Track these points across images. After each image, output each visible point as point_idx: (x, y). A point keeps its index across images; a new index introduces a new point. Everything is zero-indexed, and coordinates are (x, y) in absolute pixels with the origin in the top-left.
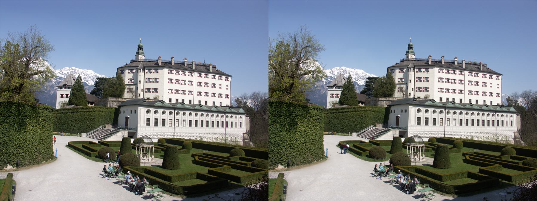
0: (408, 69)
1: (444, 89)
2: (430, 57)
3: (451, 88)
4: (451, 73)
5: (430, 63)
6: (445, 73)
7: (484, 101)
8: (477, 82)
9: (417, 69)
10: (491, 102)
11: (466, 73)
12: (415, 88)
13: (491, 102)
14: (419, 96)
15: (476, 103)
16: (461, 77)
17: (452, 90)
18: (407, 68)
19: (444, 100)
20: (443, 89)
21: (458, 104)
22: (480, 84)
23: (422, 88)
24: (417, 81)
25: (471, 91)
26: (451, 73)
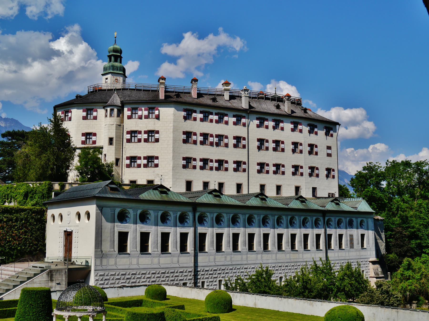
0: (107, 110)
1: (198, 160)
2: (161, 81)
3: (214, 158)
7: (297, 189)
9: (128, 110)
10: (314, 189)
12: (124, 157)
13: (314, 189)
14: (133, 179)
15: (278, 193)
16: (240, 131)
18: (104, 108)
19: (197, 187)
21: (232, 196)
23: (142, 158)
24: (129, 141)
25: (262, 165)
26: (214, 121)
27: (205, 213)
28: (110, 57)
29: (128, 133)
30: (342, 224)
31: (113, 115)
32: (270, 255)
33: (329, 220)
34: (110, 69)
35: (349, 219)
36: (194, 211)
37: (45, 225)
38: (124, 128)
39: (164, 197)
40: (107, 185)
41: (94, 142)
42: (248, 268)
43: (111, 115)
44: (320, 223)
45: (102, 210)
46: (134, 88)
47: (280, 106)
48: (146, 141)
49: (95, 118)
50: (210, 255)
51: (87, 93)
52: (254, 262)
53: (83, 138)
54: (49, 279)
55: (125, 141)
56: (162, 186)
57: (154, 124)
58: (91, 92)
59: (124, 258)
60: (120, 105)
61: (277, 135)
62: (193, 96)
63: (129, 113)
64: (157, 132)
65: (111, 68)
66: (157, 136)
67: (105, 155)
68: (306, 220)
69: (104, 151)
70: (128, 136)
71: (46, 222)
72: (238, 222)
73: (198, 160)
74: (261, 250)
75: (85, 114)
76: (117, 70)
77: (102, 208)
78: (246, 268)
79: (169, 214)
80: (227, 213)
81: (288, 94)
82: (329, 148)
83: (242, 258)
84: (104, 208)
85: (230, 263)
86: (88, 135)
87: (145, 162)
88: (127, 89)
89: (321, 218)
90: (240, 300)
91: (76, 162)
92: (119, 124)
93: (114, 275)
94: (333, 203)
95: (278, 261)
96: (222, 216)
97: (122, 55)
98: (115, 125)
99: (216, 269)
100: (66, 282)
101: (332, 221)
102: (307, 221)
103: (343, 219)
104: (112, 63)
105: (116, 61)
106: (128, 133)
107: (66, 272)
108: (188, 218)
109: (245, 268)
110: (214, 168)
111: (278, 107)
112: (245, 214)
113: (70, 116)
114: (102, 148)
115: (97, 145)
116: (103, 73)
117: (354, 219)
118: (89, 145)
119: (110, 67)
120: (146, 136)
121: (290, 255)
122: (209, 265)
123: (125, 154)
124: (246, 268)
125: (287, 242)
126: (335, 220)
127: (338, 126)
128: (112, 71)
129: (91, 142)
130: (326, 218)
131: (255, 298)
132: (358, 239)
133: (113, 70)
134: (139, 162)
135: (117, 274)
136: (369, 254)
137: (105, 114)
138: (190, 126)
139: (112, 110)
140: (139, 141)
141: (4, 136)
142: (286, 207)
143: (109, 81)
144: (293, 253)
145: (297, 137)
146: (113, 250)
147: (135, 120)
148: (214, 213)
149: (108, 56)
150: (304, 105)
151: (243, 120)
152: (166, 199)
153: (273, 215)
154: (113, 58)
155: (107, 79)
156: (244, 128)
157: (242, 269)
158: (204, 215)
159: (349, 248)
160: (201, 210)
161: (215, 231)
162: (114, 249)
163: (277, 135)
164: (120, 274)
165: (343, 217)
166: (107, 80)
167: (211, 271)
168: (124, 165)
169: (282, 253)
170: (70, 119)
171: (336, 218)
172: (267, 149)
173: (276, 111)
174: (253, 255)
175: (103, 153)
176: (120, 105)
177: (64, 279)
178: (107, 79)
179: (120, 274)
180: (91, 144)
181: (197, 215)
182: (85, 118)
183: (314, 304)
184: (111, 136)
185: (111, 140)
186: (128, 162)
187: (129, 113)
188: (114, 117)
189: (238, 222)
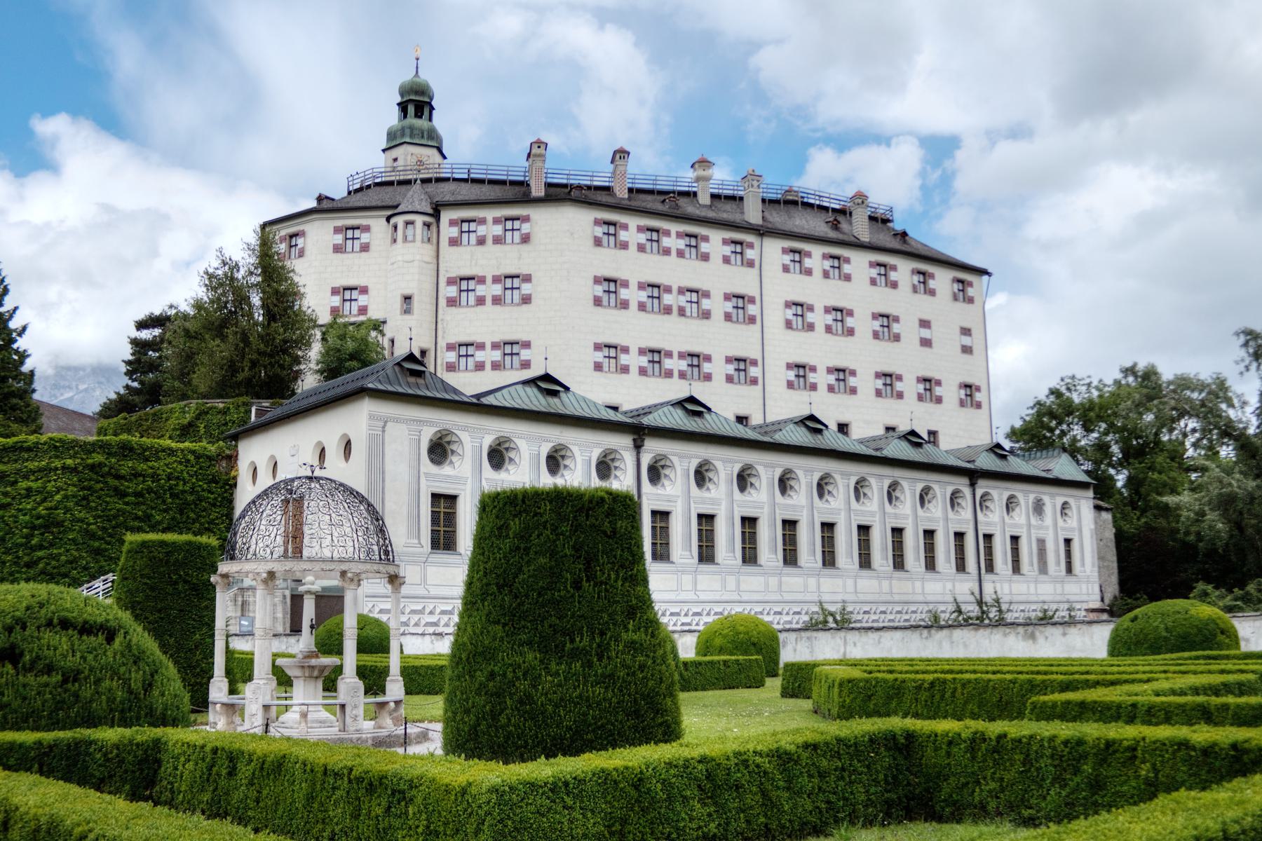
0: (396, 227)
1: (634, 351)
3: (676, 348)
4: (674, 252)
5: (538, 190)
6: (633, 248)
8: (840, 312)
9: (452, 223)
11: (773, 252)
12: (442, 344)
16: (743, 281)
17: (682, 356)
18: (388, 219)
20: (626, 350)
22: (862, 323)
23: (488, 346)
24: (452, 302)
25: (801, 369)
26: (674, 252)
27: (665, 457)
28: (403, 107)
29: (451, 282)
30: (1017, 510)
31: (410, 238)
32: (839, 582)
33: (985, 496)
34: (403, 135)
35: (1035, 498)
36: (638, 447)
37: (232, 494)
38: (440, 269)
39: (554, 405)
40: (398, 364)
41: (363, 310)
42: (785, 612)
43: (405, 239)
44: (963, 504)
45: (384, 427)
46: (465, 176)
47: (839, 222)
48: (497, 300)
49: (365, 248)
50: (683, 572)
51: (345, 194)
52: (799, 597)
53: (336, 301)
54: (239, 614)
55: (442, 302)
56: (547, 378)
57: (519, 258)
58: (357, 191)
59: (446, 565)
60: (430, 211)
61: (835, 293)
62: (618, 193)
63: (454, 232)
64: (527, 279)
65: (408, 132)
66: (526, 288)
67: (392, 341)
68: (927, 494)
69: (389, 330)
70: (452, 291)
71: (235, 485)
72: (756, 488)
73: (634, 351)
74: (815, 565)
75: (339, 239)
76: (423, 137)
77: (386, 422)
78: (780, 613)
79: (569, 454)
80: (724, 461)
81: (859, 192)
82: (966, 332)
83: (767, 585)
84: (389, 424)
85: (735, 597)
86: (345, 291)
87: (497, 355)
88: (446, 180)
89: (967, 491)
90: (795, 650)
91: (315, 351)
92: (428, 259)
93: (421, 612)
94: (993, 456)
95: (862, 597)
96: (712, 467)
97: (433, 103)
98: (416, 263)
99: (699, 610)
100: (284, 624)
101: (992, 500)
102: (930, 496)
103: (1020, 496)
104: (412, 120)
105: (419, 115)
106: (451, 282)
107: (284, 597)
108: (622, 466)
109: (776, 613)
110: (676, 374)
111: (835, 226)
112: (773, 466)
113: (299, 246)
114: (384, 322)
115: (374, 314)
116: (384, 146)
117: (1046, 499)
118: (351, 315)
119: (403, 129)
120: (497, 289)
121: (891, 584)
122: (680, 598)
123: (443, 337)
124: (780, 613)
125: (885, 549)
126: (1001, 499)
127: (985, 278)
128: (408, 140)
129: (355, 310)
130: (979, 492)
131: (845, 640)
132: (1057, 551)
133: (412, 136)
134: (480, 356)
135: (428, 610)
136: (1084, 591)
137: (392, 235)
138: (610, 262)
139: (407, 223)
140: (481, 301)
141: (141, 325)
142: (878, 454)
143: (400, 162)
144: (900, 579)
145: (884, 300)
146: (416, 541)
147: (469, 248)
148: (690, 457)
149: (399, 104)
150: (898, 226)
151: (750, 254)
152: (562, 410)
153: (846, 475)
154: (411, 109)
155: (395, 160)
156: (750, 270)
157: (768, 614)
158: (662, 463)
159: (1037, 572)
160: (653, 447)
161: (696, 508)
162: (419, 538)
163: (835, 293)
164: (438, 611)
165: (1022, 491)
166: (395, 165)
167: (686, 615)
168: (442, 365)
169: (871, 578)
170: (301, 254)
171: (1001, 495)
172: (811, 327)
173: (832, 234)
174: (796, 579)
175: (389, 335)
176: (430, 211)
177: (280, 615)
178: (395, 160)
179: (438, 611)
180: (355, 316)
181: (646, 460)
182: (338, 249)
183: (1037, 634)
184: (407, 292)
185: (407, 299)
186: (451, 357)
187: (454, 232)
188: (414, 241)
189: (756, 488)
